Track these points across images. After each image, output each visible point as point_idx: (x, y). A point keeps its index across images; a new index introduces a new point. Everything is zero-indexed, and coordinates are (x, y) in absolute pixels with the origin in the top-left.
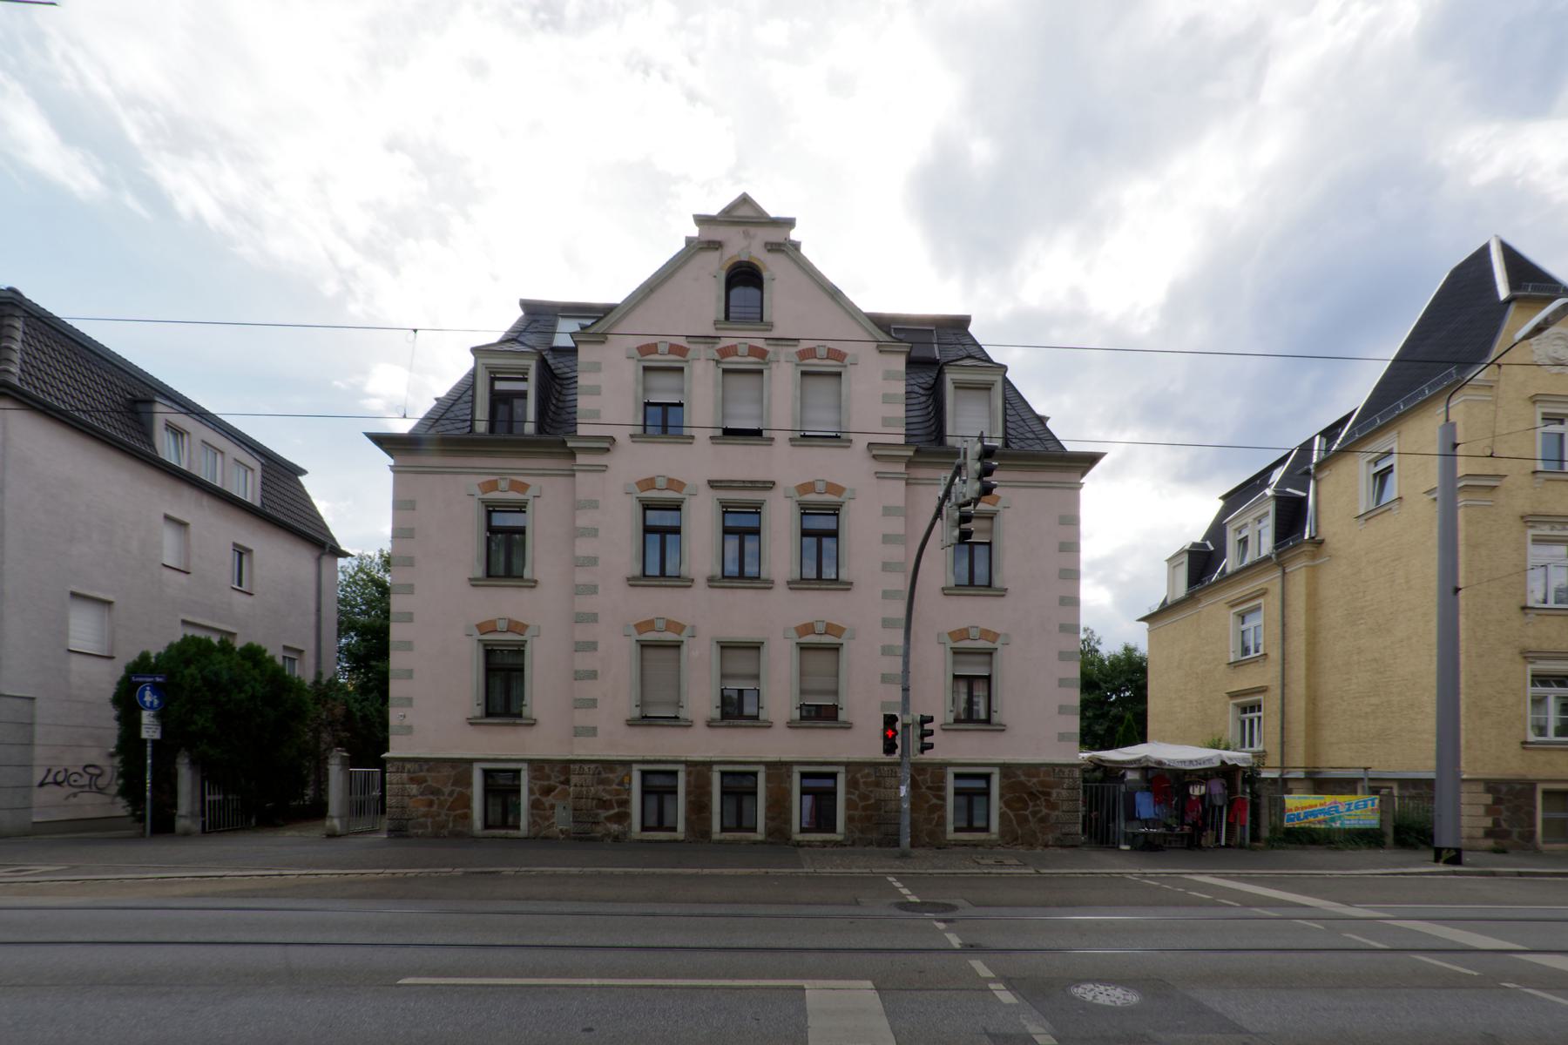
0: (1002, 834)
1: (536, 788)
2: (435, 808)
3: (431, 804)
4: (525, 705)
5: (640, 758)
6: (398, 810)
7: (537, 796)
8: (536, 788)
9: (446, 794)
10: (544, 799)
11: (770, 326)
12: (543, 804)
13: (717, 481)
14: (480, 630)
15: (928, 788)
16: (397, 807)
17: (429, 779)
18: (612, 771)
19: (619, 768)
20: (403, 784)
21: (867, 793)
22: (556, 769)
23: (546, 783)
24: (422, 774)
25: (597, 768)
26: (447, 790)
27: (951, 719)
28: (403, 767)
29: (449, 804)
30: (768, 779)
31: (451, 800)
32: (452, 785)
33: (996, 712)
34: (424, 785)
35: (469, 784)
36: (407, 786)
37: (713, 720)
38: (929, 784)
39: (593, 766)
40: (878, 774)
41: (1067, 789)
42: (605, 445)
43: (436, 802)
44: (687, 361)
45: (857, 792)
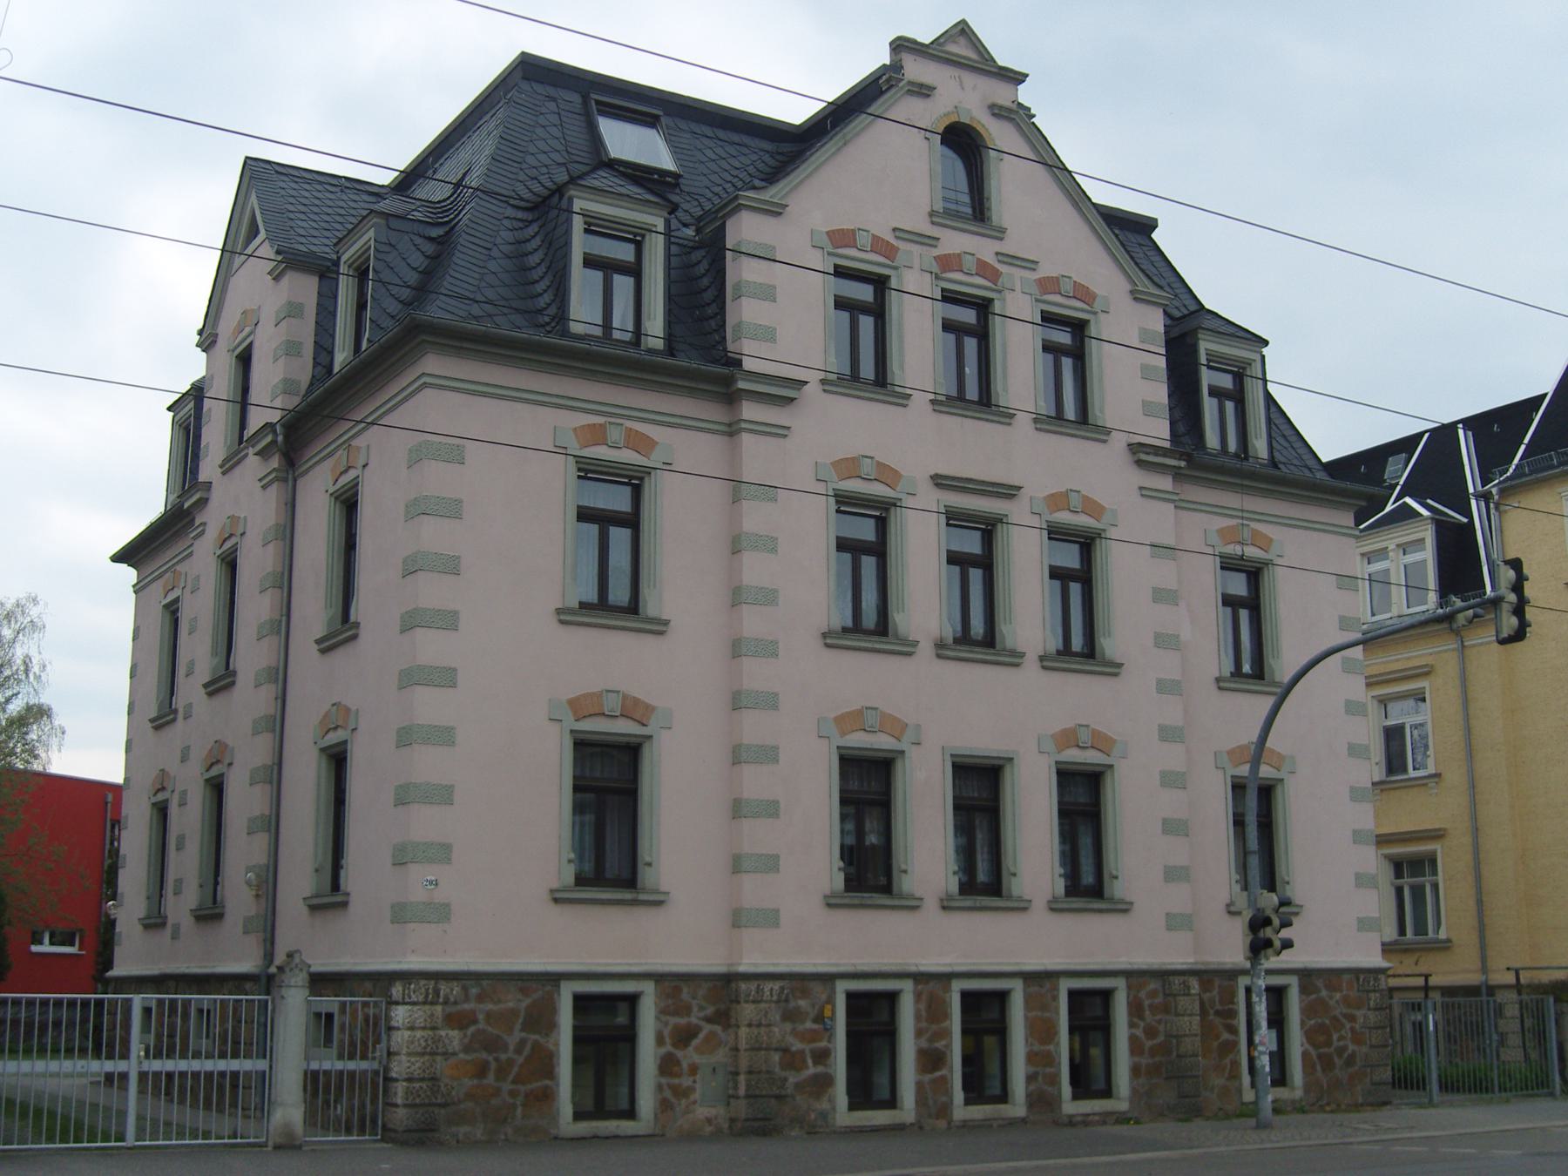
0: (1307, 1088)
1: (666, 1033)
2: (490, 1079)
3: (482, 1071)
4: (955, 873)
5: (850, 969)
6: (424, 1085)
7: (668, 1048)
8: (666, 1033)
9: (511, 1048)
10: (679, 1054)
11: (999, 233)
12: (678, 1063)
13: (947, 477)
14: (575, 712)
15: (1217, 1013)
16: (422, 1080)
17: (481, 1017)
18: (805, 993)
19: (818, 989)
20: (433, 1028)
21: (1154, 1023)
22: (701, 993)
23: (682, 1021)
24: (466, 1006)
25: (782, 989)
26: (512, 1040)
27: (569, 878)
28: (437, 992)
29: (516, 1069)
30: (1028, 1000)
31: (520, 1060)
32: (522, 1030)
33: (649, 864)
34: (472, 1029)
35: (551, 1026)
36: (443, 1033)
37: (949, 897)
38: (1218, 1007)
39: (777, 985)
40: (1167, 992)
41: (1376, 1009)
42: (783, 392)
43: (493, 1065)
44: (896, 268)
45: (1142, 1024)
